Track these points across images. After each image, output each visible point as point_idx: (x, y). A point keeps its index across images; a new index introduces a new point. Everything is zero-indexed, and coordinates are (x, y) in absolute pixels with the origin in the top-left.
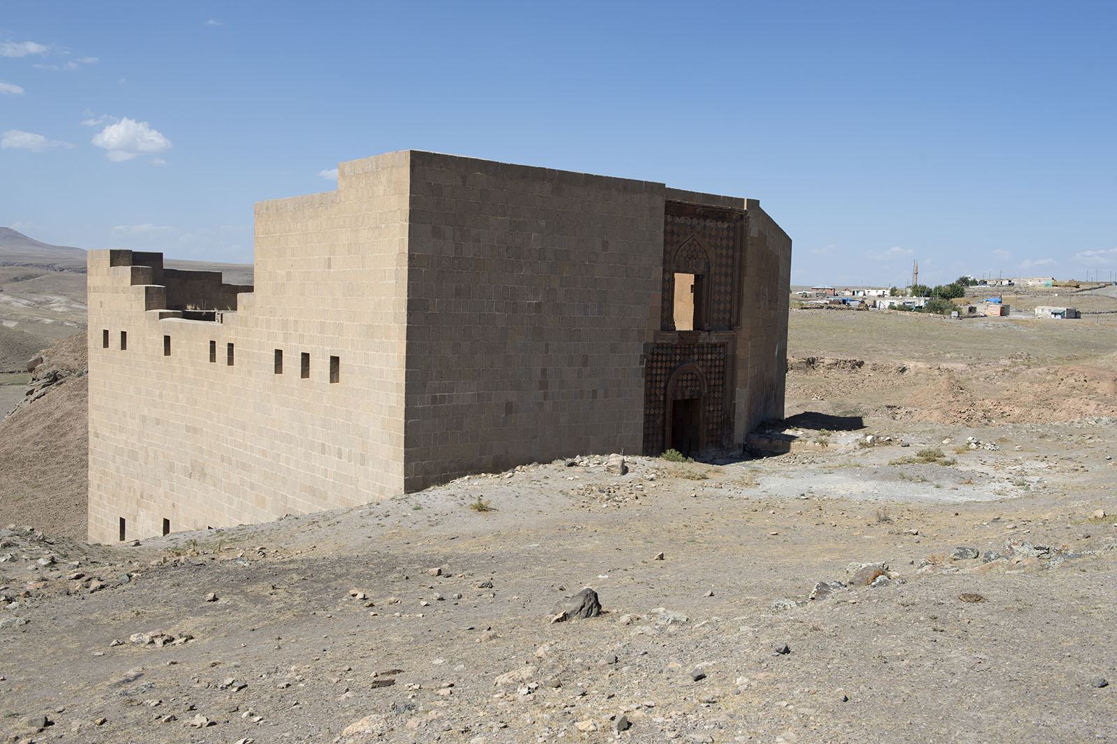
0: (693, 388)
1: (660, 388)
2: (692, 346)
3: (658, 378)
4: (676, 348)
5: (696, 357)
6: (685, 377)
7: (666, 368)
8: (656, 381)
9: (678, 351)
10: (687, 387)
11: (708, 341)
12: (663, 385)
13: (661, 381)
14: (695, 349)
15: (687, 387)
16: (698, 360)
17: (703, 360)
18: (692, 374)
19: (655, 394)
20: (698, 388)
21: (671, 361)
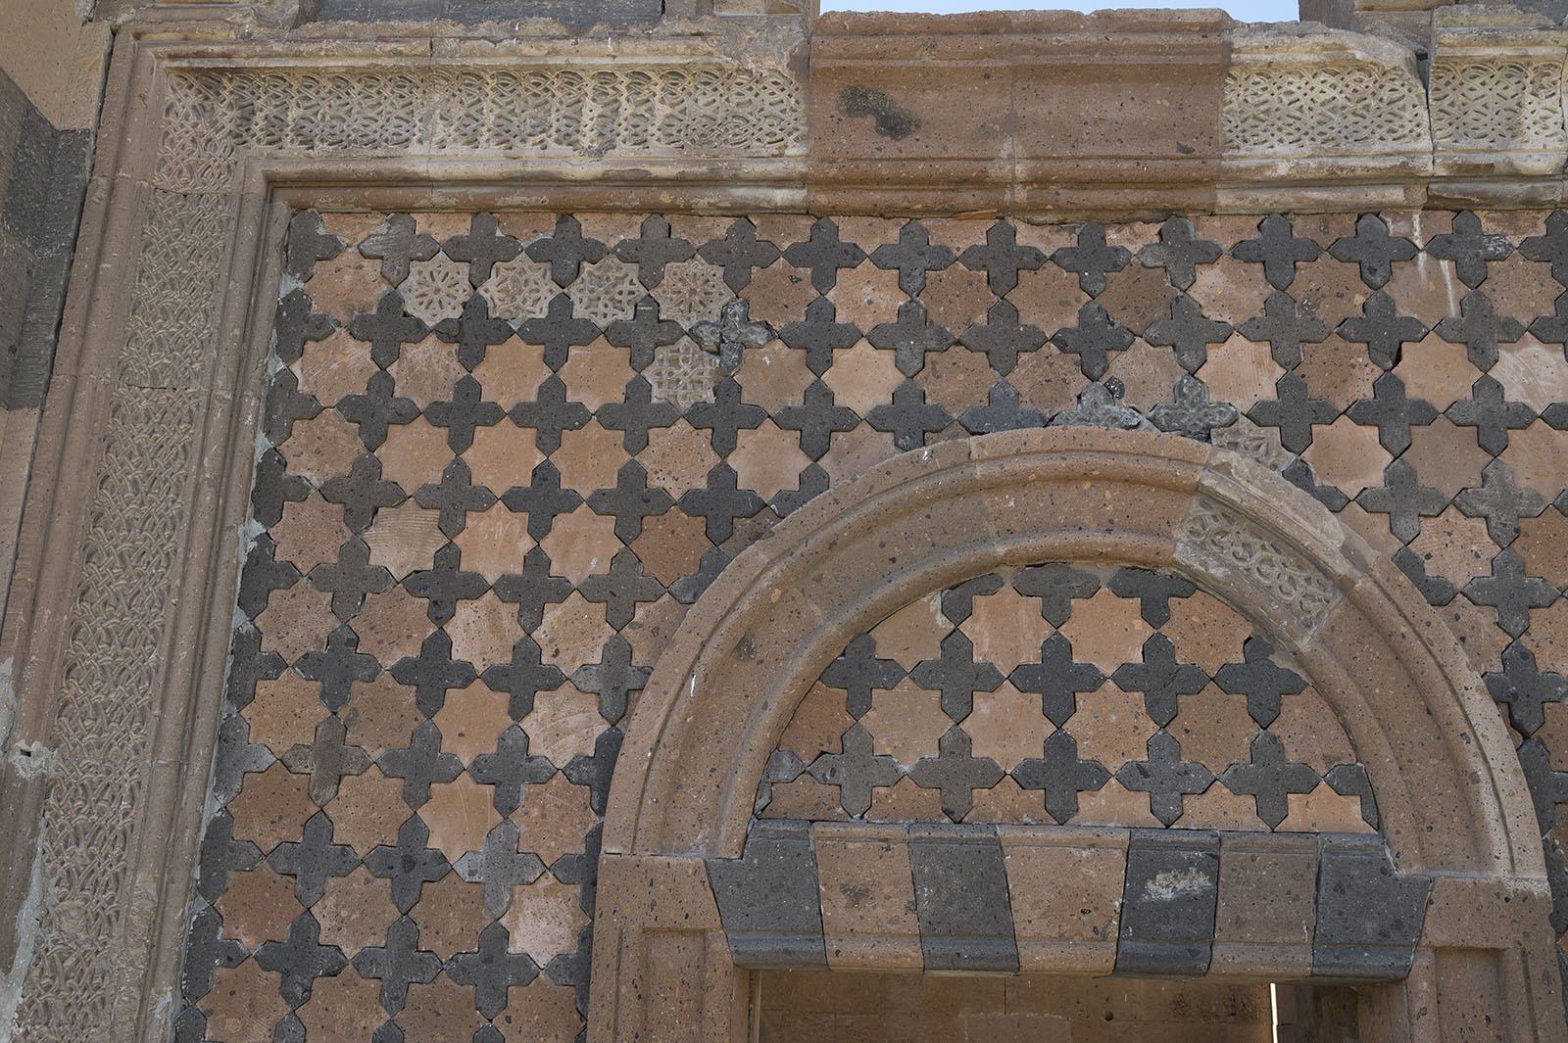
0: (1222, 810)
1: (508, 773)
2: (1135, 241)
3: (476, 634)
4: (827, 258)
5: (1242, 373)
6: (1007, 629)
7: (632, 503)
8: (434, 673)
9: (866, 296)
10: (1061, 777)
11: (1424, 142)
12: (561, 729)
13: (525, 678)
14: (1209, 282)
15: (1061, 777)
16: (1294, 416)
17: (1389, 410)
18: (1154, 588)
19: (409, 864)
20: (1326, 812)
21: (725, 418)
